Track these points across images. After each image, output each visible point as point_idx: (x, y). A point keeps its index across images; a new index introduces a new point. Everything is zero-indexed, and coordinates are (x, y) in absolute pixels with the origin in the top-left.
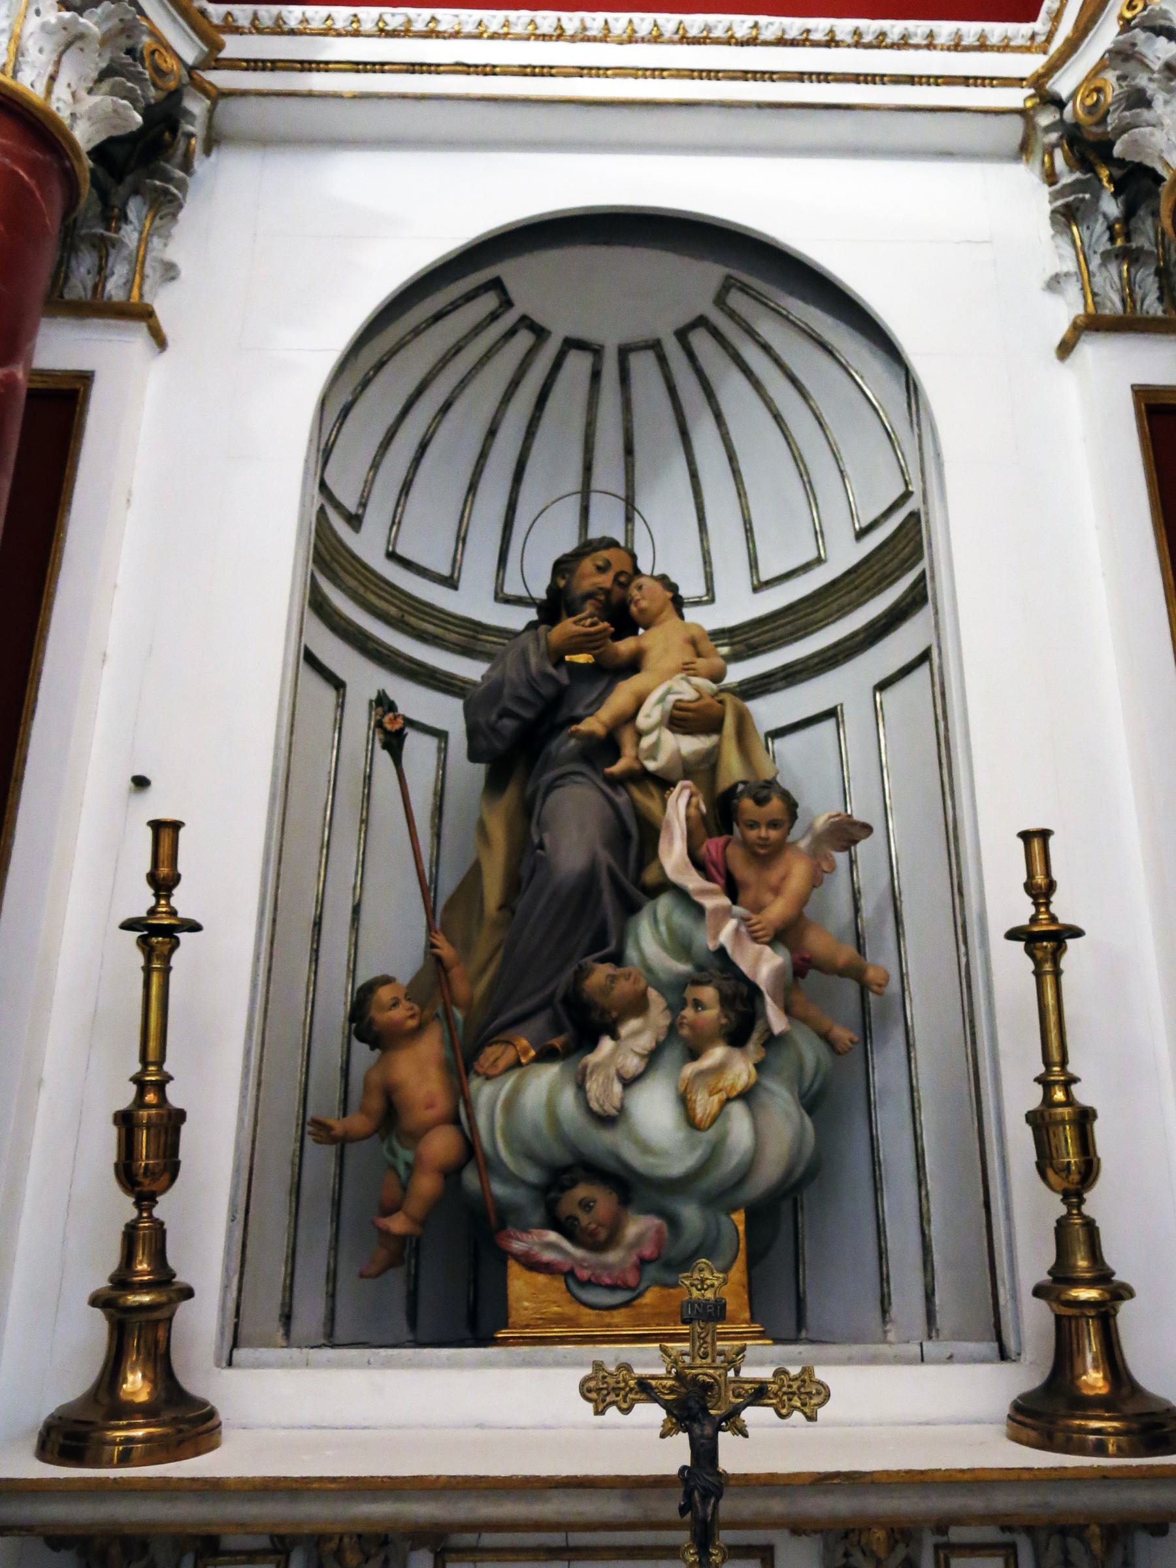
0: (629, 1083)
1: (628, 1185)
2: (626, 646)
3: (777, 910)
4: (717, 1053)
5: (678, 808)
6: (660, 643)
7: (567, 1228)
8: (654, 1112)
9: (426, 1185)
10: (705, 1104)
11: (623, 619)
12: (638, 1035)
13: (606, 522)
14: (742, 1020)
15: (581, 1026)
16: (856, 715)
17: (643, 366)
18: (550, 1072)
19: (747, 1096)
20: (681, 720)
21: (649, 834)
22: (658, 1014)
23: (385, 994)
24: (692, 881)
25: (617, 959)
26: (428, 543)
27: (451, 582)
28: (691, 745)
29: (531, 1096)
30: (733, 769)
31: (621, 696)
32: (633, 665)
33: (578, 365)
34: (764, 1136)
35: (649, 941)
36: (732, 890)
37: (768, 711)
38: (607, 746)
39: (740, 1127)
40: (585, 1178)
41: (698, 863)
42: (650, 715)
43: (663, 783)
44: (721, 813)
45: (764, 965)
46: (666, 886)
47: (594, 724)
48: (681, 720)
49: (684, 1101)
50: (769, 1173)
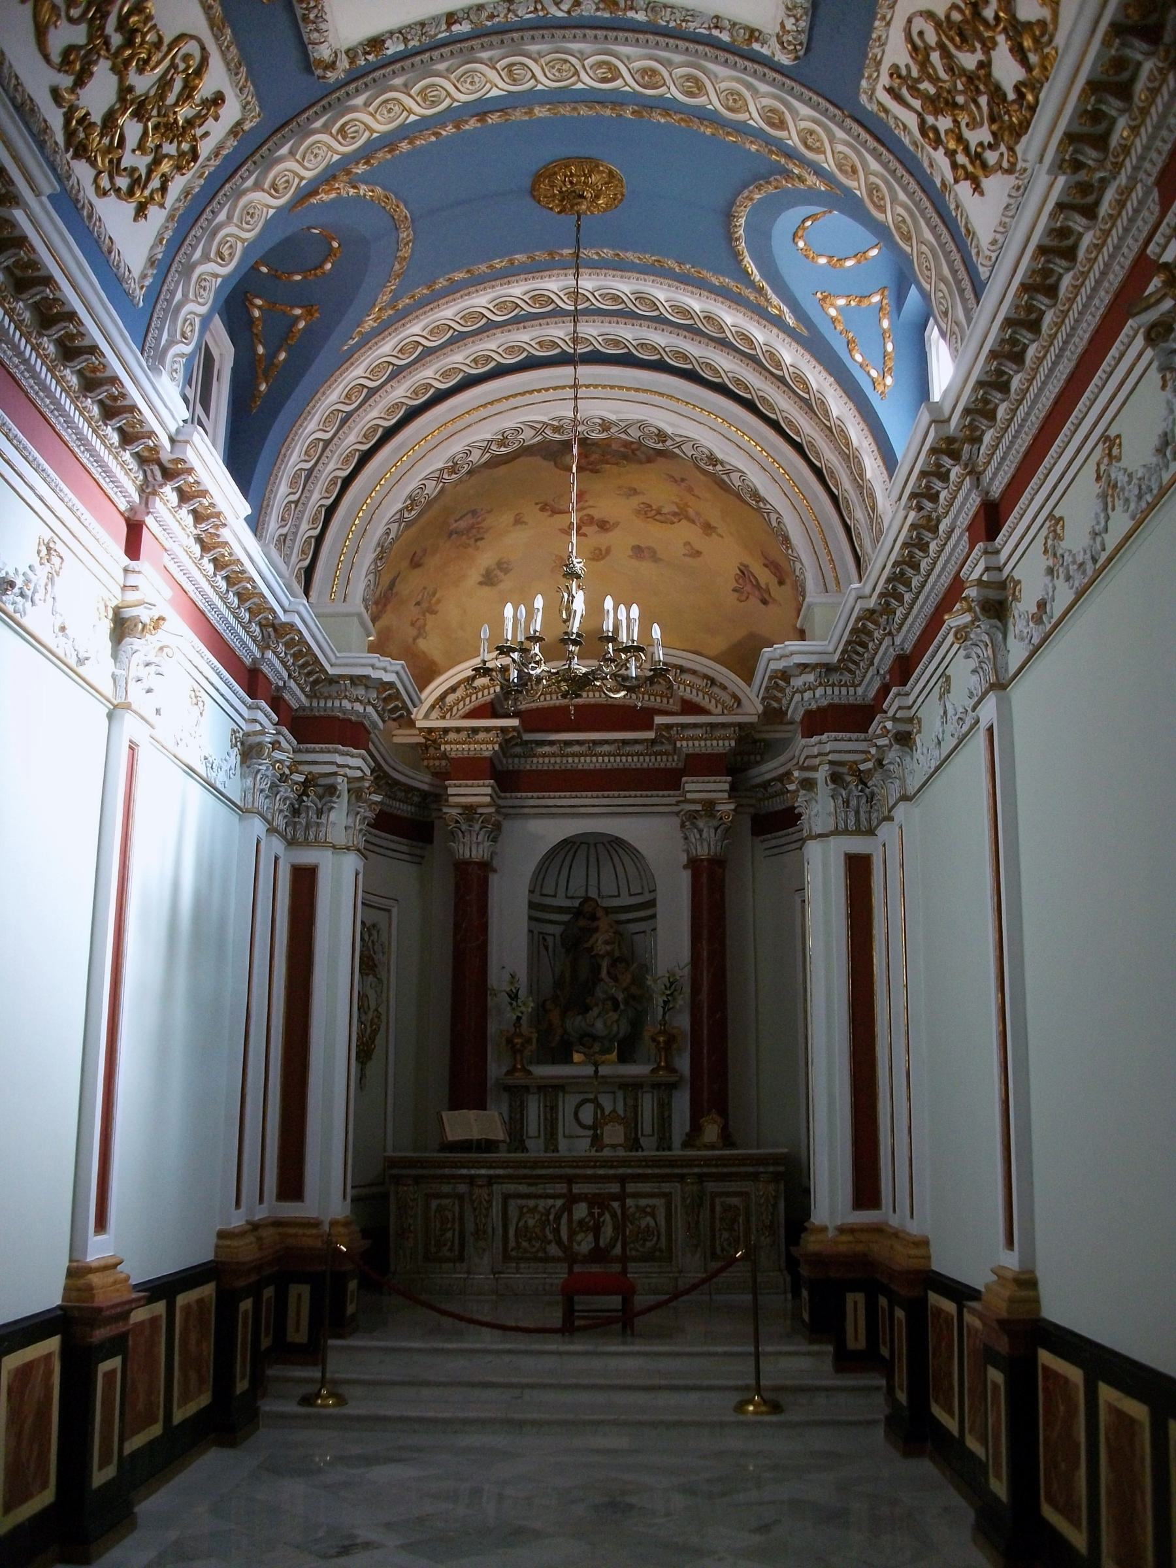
0: (595, 1019)
1: (595, 1038)
2: (595, 924)
3: (625, 985)
4: (611, 1014)
5: (605, 964)
6: (603, 923)
7: (583, 1045)
8: (599, 1025)
9: (557, 1038)
10: (609, 1023)
11: (594, 917)
12: (595, 1011)
13: (593, 893)
14: (616, 1007)
15: (586, 1009)
16: (648, 932)
17: (600, 848)
18: (580, 1017)
19: (617, 1021)
20: (606, 943)
21: (599, 967)
22: (600, 1006)
23: (548, 1002)
24: (607, 979)
25: (593, 995)
26: (549, 890)
27: (554, 896)
28: (609, 948)
29: (576, 1023)
30: (617, 954)
31: (595, 936)
32: (597, 929)
33: (584, 846)
34: (624, 1029)
35: (599, 993)
36: (615, 979)
37: (634, 928)
38: (592, 949)
39: (615, 1028)
40: (587, 1039)
41: (608, 973)
42: (600, 942)
43: (603, 957)
44: (614, 962)
45: (620, 997)
46: (602, 980)
47: (586, 945)
48: (606, 943)
49: (605, 1023)
50: (621, 1035)
